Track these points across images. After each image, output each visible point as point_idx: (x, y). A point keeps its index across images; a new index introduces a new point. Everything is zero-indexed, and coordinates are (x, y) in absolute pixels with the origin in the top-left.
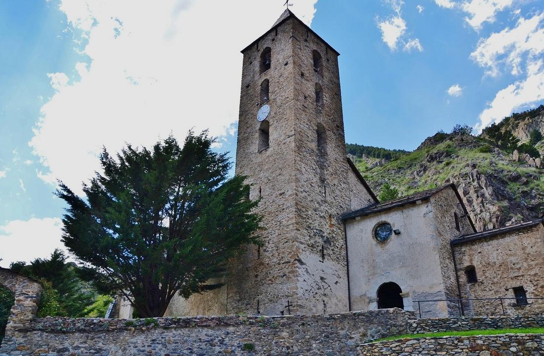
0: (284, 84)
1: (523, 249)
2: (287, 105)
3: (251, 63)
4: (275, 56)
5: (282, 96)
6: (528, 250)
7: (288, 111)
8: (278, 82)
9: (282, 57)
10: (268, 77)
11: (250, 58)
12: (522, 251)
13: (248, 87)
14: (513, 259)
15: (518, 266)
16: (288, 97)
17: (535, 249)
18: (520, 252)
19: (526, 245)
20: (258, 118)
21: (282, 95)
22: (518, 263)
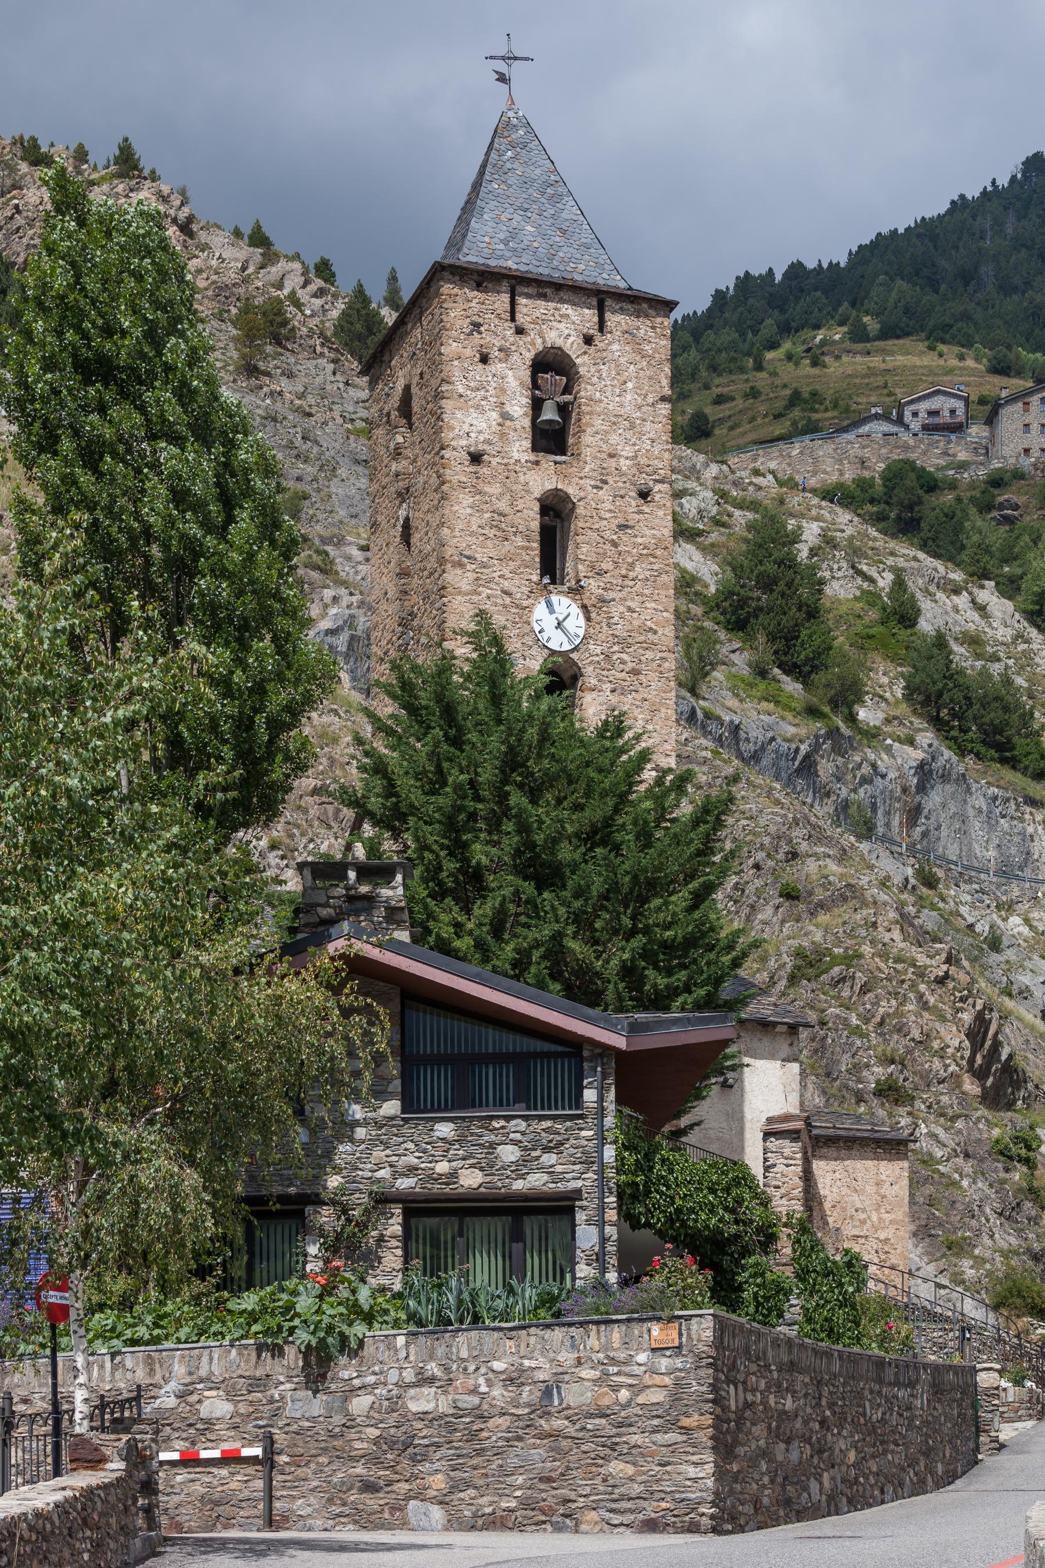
0: (638, 569)
1: (877, 1184)
2: (649, 655)
3: (484, 359)
4: (598, 422)
5: (631, 610)
6: (886, 1189)
7: (654, 676)
8: (615, 544)
9: (628, 451)
10: (570, 491)
11: (477, 326)
12: (875, 1188)
13: (476, 458)
14: (857, 1200)
15: (862, 1216)
16: (655, 632)
17: (895, 1187)
18: (870, 1189)
19: (883, 1177)
20: (537, 629)
21: (629, 603)
22: (864, 1210)
